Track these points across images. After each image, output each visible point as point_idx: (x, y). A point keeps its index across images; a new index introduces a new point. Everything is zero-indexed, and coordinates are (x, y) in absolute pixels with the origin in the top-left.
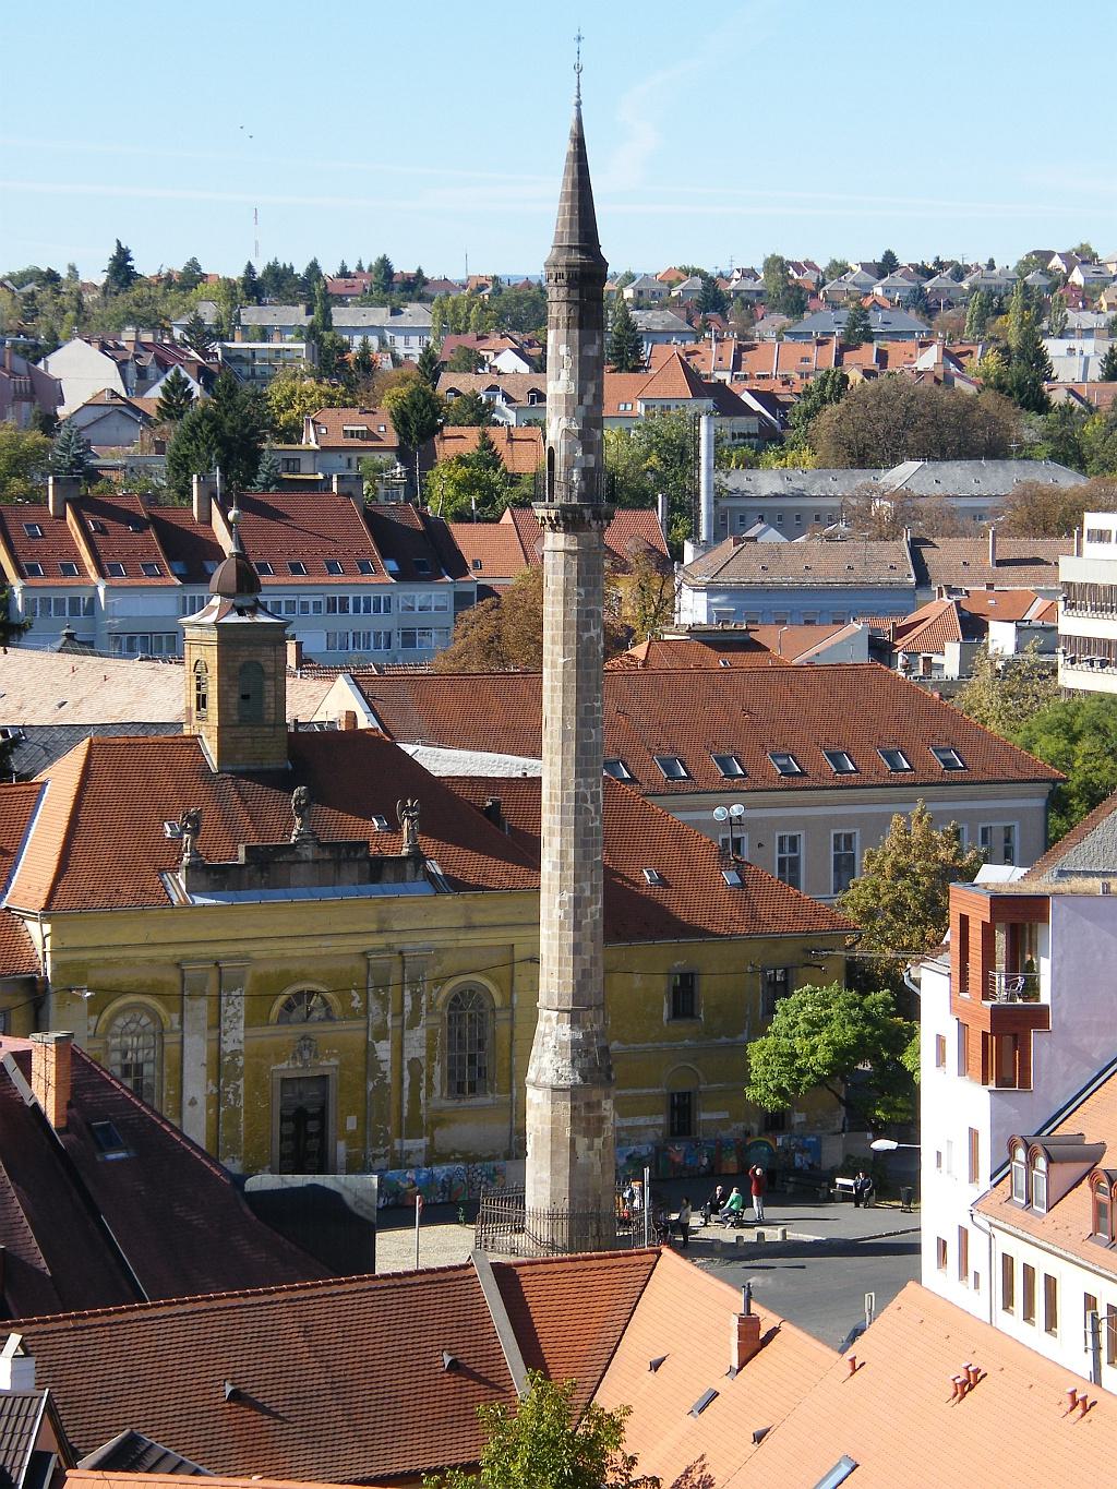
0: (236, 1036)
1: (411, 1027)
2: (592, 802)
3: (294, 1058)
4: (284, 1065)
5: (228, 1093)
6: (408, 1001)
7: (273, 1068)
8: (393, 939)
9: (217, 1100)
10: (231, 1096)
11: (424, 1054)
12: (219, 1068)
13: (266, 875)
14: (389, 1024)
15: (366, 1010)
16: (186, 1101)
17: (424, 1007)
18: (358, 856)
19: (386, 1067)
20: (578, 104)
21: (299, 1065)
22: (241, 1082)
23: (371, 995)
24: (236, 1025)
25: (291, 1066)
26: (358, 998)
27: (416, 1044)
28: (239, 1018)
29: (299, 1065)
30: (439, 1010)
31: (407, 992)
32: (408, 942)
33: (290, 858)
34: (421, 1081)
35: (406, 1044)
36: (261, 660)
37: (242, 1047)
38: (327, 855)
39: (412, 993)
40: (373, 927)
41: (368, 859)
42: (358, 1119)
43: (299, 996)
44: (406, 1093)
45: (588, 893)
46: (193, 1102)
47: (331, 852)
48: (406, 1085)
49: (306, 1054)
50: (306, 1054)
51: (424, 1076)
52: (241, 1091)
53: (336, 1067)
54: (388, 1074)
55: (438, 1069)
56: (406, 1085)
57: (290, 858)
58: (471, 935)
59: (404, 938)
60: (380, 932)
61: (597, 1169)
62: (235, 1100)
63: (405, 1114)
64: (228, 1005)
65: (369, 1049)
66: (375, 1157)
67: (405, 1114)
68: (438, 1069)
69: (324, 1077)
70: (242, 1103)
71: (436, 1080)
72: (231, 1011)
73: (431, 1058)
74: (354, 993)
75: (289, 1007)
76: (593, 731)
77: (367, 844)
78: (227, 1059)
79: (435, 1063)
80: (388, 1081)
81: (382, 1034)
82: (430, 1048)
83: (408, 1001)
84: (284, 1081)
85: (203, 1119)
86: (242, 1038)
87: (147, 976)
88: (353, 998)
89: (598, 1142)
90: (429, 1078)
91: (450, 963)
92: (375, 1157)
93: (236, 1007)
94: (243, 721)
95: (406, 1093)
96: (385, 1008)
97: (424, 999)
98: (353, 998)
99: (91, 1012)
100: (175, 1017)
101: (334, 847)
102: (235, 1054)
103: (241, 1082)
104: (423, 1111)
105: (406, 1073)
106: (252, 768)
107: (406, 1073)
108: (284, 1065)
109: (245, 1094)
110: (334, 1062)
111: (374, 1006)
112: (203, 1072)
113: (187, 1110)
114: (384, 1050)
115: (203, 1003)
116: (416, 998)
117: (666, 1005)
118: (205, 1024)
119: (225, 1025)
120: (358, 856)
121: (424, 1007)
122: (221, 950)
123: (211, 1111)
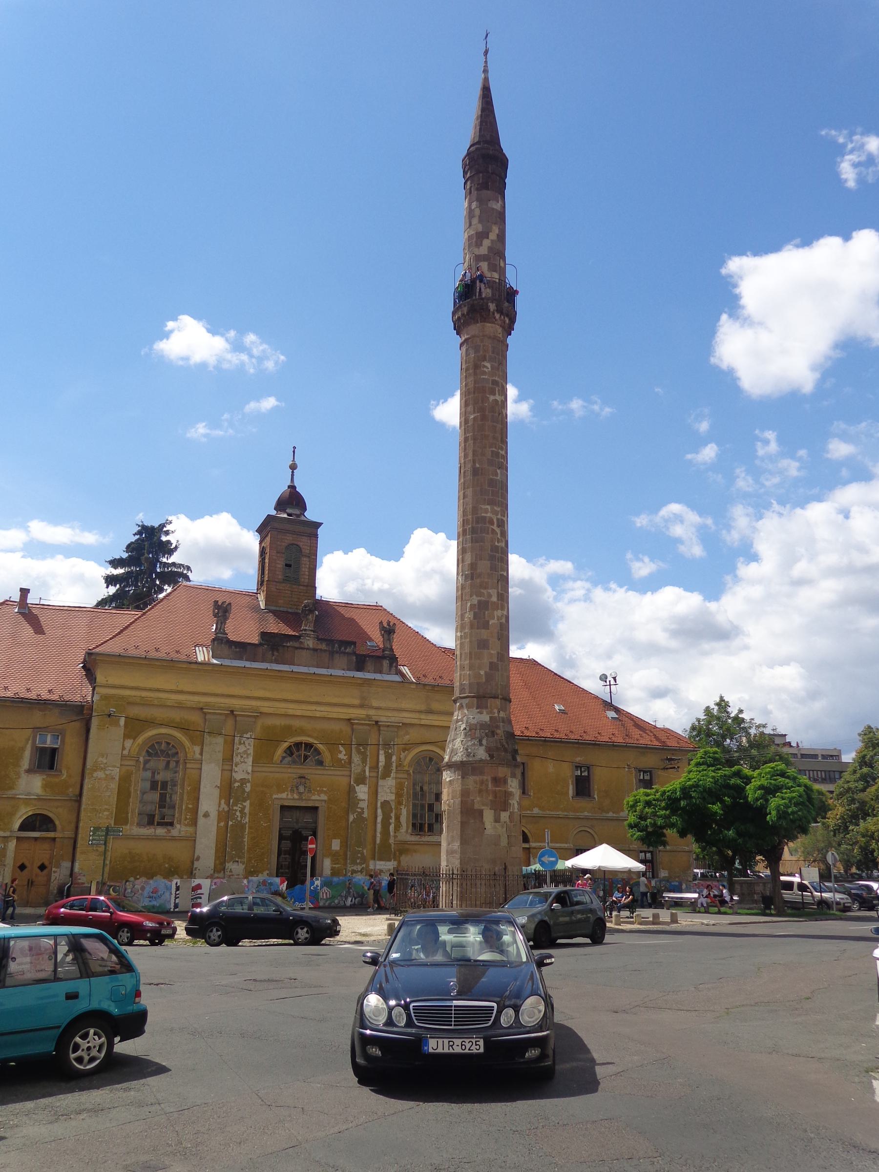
0: (244, 769)
1: (384, 778)
2: (498, 526)
3: (292, 791)
4: (284, 795)
5: (236, 810)
6: (382, 758)
7: (275, 796)
8: (372, 712)
9: (225, 816)
10: (238, 814)
11: (393, 798)
12: (229, 791)
13: (276, 653)
14: (367, 774)
15: (350, 762)
16: (201, 813)
17: (394, 765)
18: (347, 650)
19: (363, 805)
20: (485, 71)
21: (296, 796)
22: (247, 804)
23: (354, 750)
24: (246, 760)
25: (290, 796)
26: (344, 752)
27: (388, 791)
28: (248, 755)
29: (296, 796)
30: (406, 768)
31: (382, 752)
32: (384, 717)
33: (296, 645)
34: (391, 818)
35: (379, 790)
36: (301, 544)
37: (250, 777)
38: (323, 646)
39: (385, 753)
40: (357, 702)
41: (354, 653)
42: (341, 842)
43: (298, 745)
44: (379, 826)
45: (494, 599)
46: (206, 815)
47: (327, 645)
48: (379, 819)
49: (301, 789)
50: (301, 789)
51: (393, 815)
52: (247, 810)
53: (325, 801)
54: (366, 810)
55: (404, 812)
56: (379, 819)
57: (296, 645)
58: (430, 717)
59: (380, 712)
60: (361, 706)
61: (504, 842)
62: (241, 818)
63: (378, 841)
64: (240, 743)
65: (351, 791)
66: (354, 872)
67: (378, 841)
68: (404, 812)
69: (315, 809)
70: (247, 820)
71: (403, 819)
72: (242, 749)
73: (399, 803)
74: (341, 748)
75: (289, 751)
76: (499, 471)
77: (354, 643)
78: (237, 785)
79: (402, 807)
80: (365, 815)
81: (361, 780)
82: (399, 795)
83: (382, 758)
84: (283, 807)
85: (214, 829)
86: (250, 771)
87: (176, 715)
88: (341, 752)
89: (504, 816)
90: (398, 818)
91: (413, 735)
92: (354, 872)
93: (246, 747)
94: (286, 580)
95: (379, 826)
96: (364, 761)
97: (394, 758)
98: (341, 752)
99: (126, 736)
100: (197, 749)
101: (330, 642)
102: (243, 781)
103: (247, 804)
104: (392, 841)
105: (379, 811)
106: (290, 610)
107: (379, 811)
108: (284, 795)
109: (250, 814)
110: (324, 797)
111: (356, 758)
112: (217, 792)
113: (201, 821)
114: (362, 792)
115: (220, 740)
116: (388, 757)
117: (571, 787)
118: (220, 756)
119: (237, 759)
120: (347, 650)
121: (394, 765)
122: (236, 703)
123: (222, 824)
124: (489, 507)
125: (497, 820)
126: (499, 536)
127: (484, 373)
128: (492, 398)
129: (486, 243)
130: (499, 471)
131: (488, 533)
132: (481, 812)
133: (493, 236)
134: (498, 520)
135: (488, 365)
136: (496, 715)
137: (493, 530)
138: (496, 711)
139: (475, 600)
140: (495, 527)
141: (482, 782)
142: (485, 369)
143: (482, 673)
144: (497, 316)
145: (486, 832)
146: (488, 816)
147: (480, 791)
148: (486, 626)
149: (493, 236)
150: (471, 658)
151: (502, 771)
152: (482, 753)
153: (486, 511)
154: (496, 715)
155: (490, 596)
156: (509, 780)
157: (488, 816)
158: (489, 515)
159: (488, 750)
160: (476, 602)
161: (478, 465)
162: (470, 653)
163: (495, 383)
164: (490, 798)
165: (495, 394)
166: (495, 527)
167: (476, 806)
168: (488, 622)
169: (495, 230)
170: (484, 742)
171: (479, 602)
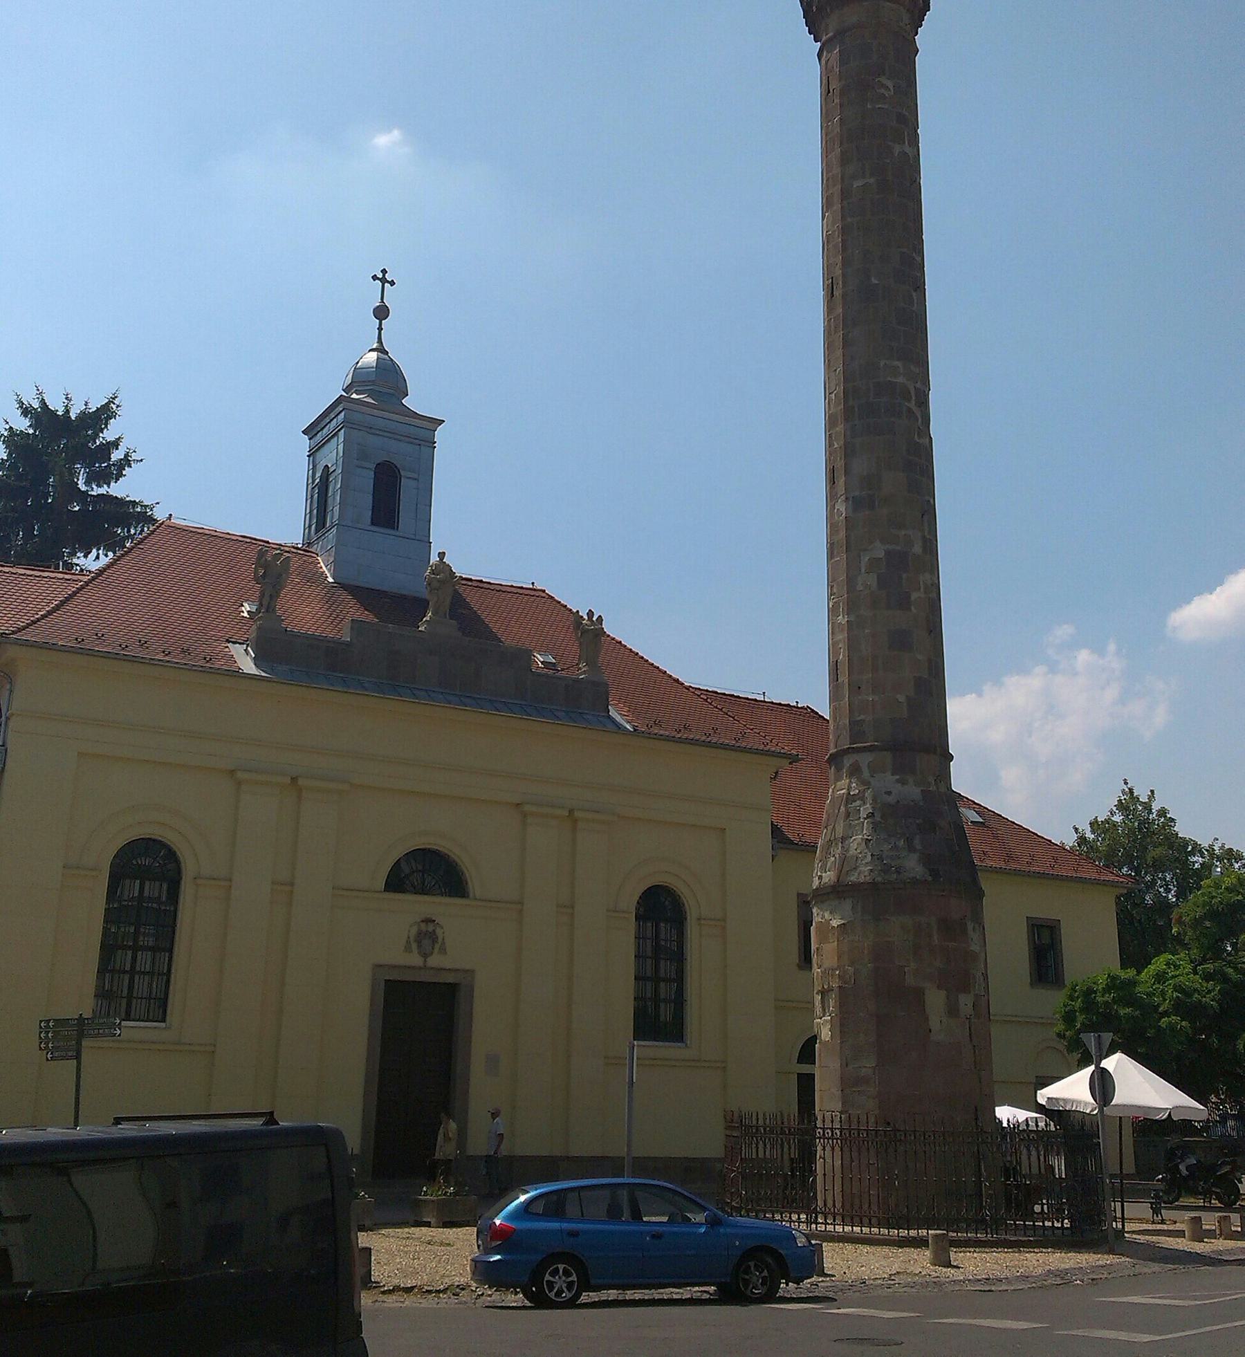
89: (965, 1002)
124: (896, 363)
125: (952, 1010)
128: (897, 149)
132: (919, 994)
135: (890, 84)
137: (910, 410)
138: (931, 779)
139: (879, 551)
140: (912, 405)
142: (882, 91)
143: (901, 698)
152: (913, 866)
158: (901, 380)
160: (881, 554)
161: (874, 281)
166: (912, 405)
167: (910, 980)
171: (888, 553)
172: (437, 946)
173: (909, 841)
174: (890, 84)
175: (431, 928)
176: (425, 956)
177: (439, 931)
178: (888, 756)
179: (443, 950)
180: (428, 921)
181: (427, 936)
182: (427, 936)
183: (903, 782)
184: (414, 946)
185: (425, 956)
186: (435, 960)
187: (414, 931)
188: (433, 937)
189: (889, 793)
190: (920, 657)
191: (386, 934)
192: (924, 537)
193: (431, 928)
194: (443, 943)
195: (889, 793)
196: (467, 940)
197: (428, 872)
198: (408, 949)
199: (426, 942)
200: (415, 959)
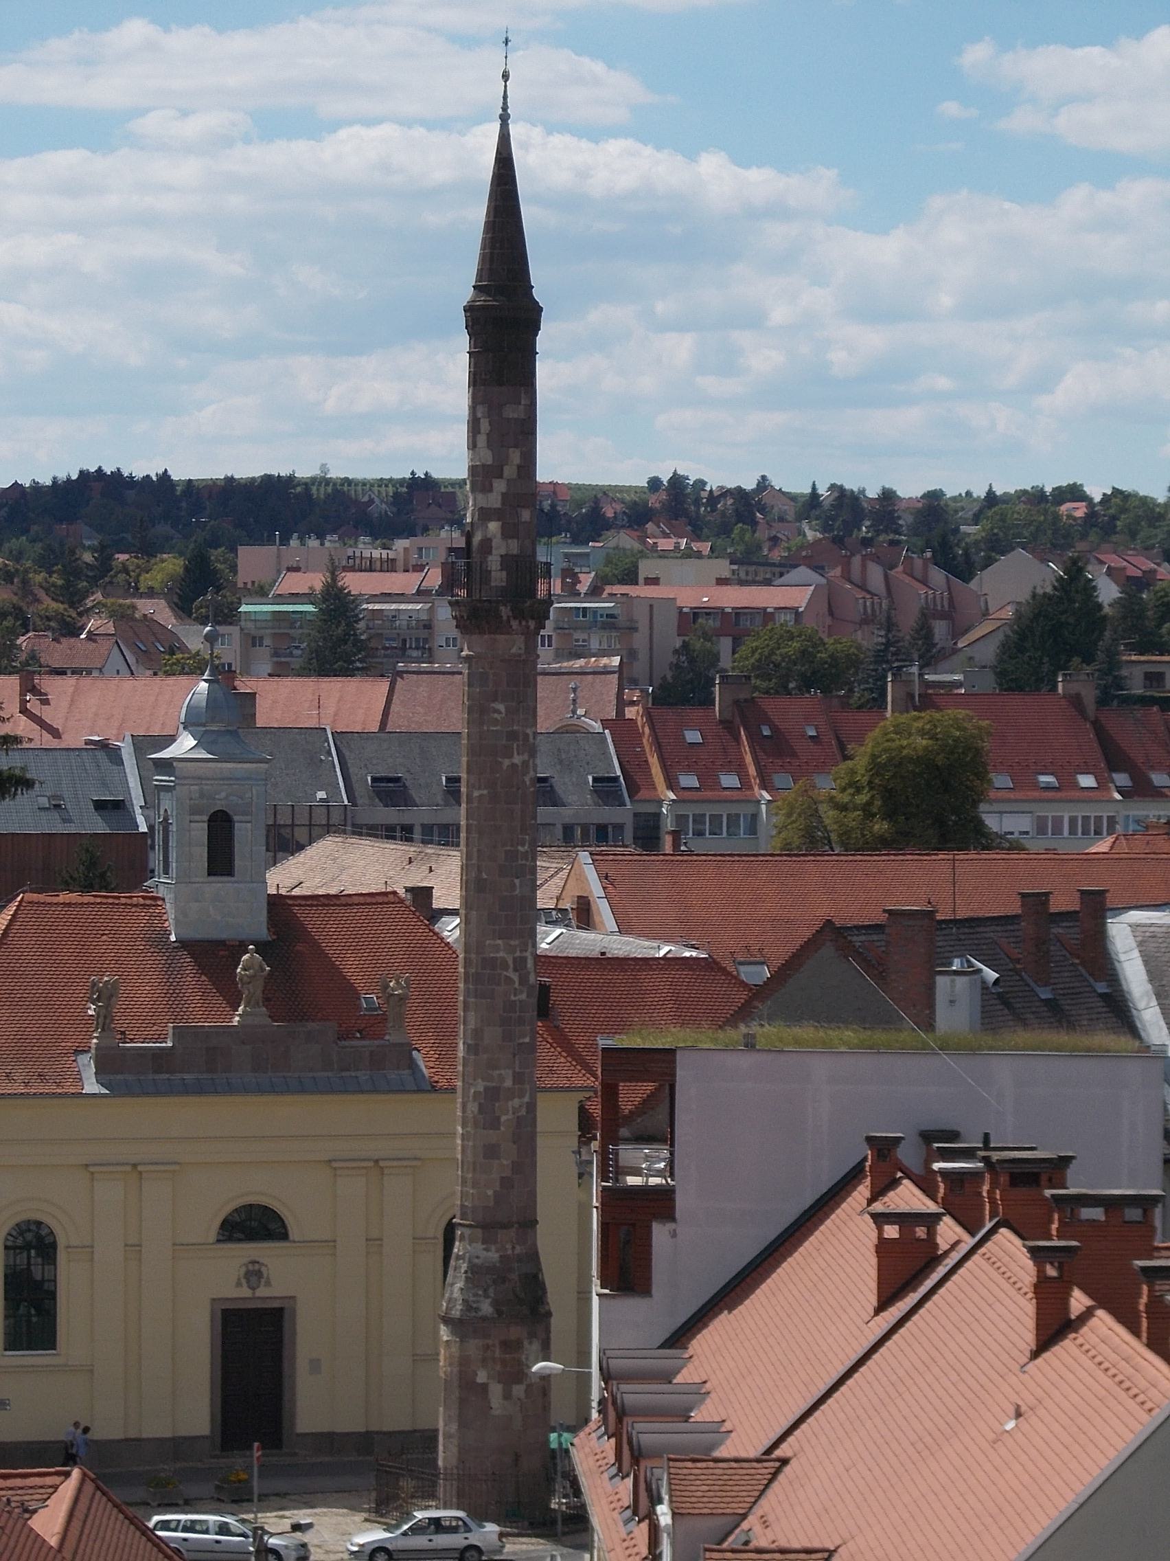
2: (515, 970)
45: (508, 1083)
76: (517, 881)
89: (518, 1390)
124: (500, 942)
125: (507, 1396)
126: (517, 985)
127: (496, 722)
128: (507, 762)
129: (500, 486)
130: (517, 881)
131: (499, 984)
132: (484, 1387)
133: (509, 471)
134: (515, 959)
135: (501, 707)
136: (509, 1252)
137: (509, 980)
138: (509, 1246)
139: (480, 1086)
141: (487, 1347)
142: (496, 715)
143: (490, 1192)
144: (515, 624)
145: (494, 1412)
146: (496, 1390)
147: (484, 1360)
148: (494, 1124)
149: (509, 471)
150: (474, 1170)
151: (515, 1332)
152: (486, 1308)
153: (497, 949)
154: (509, 1252)
155: (502, 1079)
156: (526, 1343)
157: (496, 1390)
158: (501, 954)
159: (496, 1304)
162: (474, 1163)
163: (512, 736)
164: (498, 1367)
165: (511, 757)
168: (498, 1118)
169: (515, 457)
170: (491, 1292)
171: (486, 1089)
172: (263, 1281)
173: (485, 1291)
174: (501, 707)
175: (257, 1267)
176: (253, 1289)
177: (263, 1269)
178: (479, 1232)
179: (268, 1284)
180: (254, 1262)
181: (254, 1274)
182: (254, 1274)
183: (487, 1250)
184: (244, 1281)
185: (253, 1289)
186: (262, 1292)
187: (243, 1270)
188: (259, 1274)
189: (478, 1257)
190: (505, 1162)
191: (223, 1275)
192: (514, 1072)
193: (257, 1267)
194: (268, 1278)
195: (478, 1257)
196: (285, 1273)
197: (254, 1224)
198: (239, 1284)
199: (254, 1279)
200: (245, 1292)
